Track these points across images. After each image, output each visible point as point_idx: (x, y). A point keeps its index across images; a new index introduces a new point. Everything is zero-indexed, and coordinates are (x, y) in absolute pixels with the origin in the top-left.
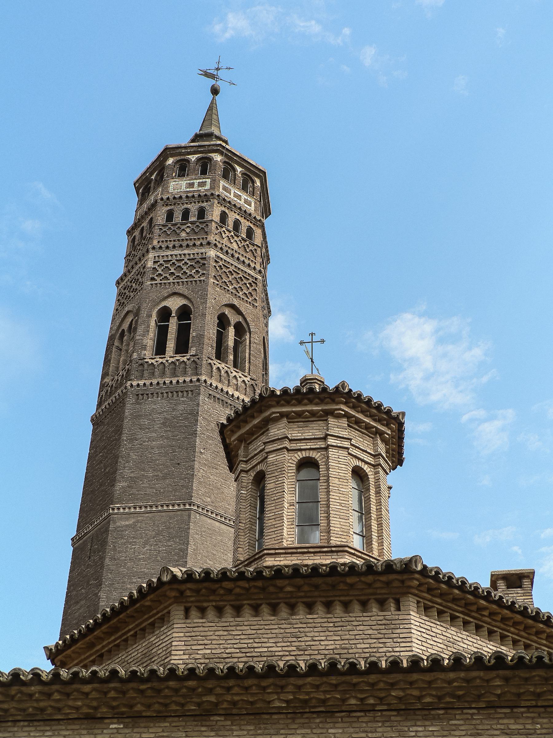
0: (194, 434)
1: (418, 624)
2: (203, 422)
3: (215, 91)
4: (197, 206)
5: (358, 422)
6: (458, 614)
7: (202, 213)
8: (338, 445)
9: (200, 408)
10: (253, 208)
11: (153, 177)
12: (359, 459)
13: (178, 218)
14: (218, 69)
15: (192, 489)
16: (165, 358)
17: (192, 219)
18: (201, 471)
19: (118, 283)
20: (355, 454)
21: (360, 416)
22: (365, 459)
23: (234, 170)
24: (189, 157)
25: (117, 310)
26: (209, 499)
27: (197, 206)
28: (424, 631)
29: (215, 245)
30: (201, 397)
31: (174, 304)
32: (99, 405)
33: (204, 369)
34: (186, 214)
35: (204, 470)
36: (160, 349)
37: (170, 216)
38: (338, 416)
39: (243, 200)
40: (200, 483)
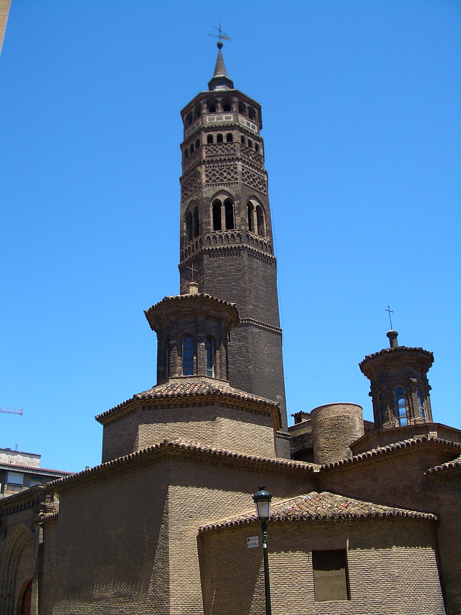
3: (220, 46)
4: (227, 132)
7: (230, 137)
10: (256, 131)
11: (193, 110)
13: (215, 141)
14: (220, 31)
16: (222, 232)
17: (225, 141)
19: (181, 179)
23: (245, 106)
24: (217, 99)
25: (183, 198)
27: (227, 132)
29: (241, 159)
31: (222, 198)
32: (182, 257)
33: (244, 239)
34: (220, 137)
36: (217, 226)
37: (210, 139)
39: (251, 126)
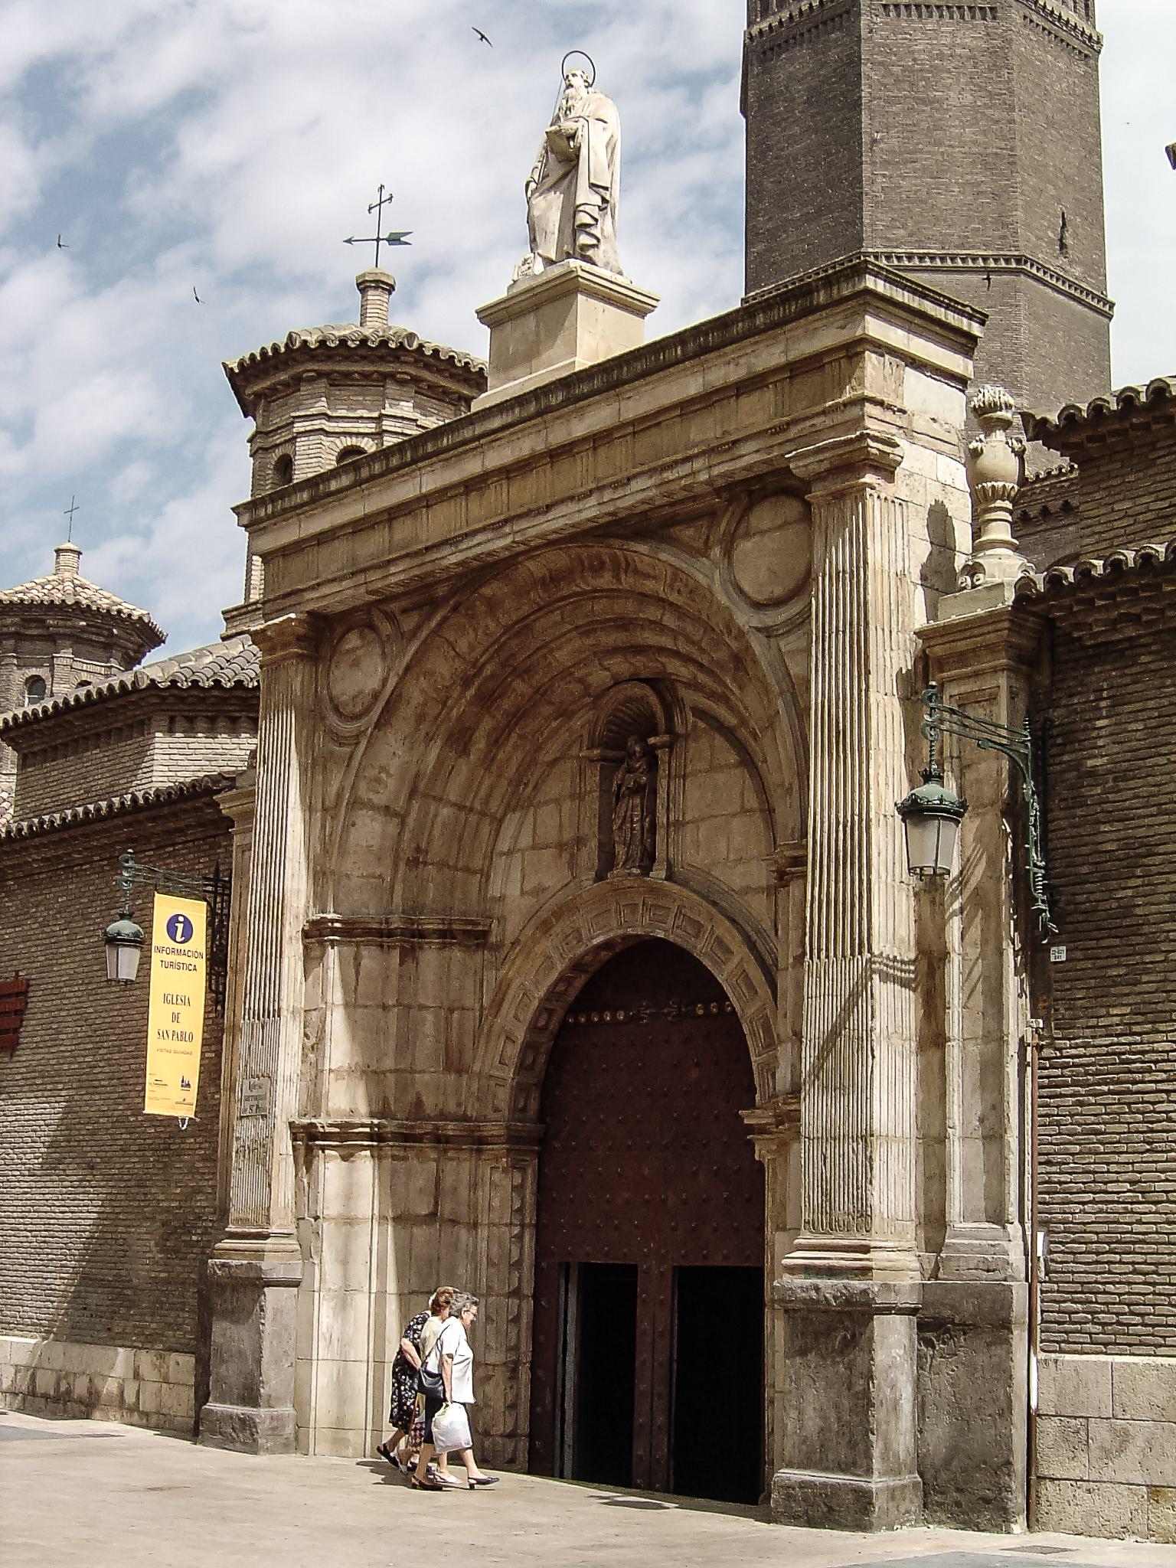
0: (857, 105)
1: (166, 746)
2: (872, 74)
5: (347, 375)
6: (237, 714)
8: (308, 428)
9: (864, 47)
12: (351, 434)
15: (862, 223)
18: (880, 179)
20: (342, 430)
21: (343, 367)
22: (361, 431)
26: (902, 232)
28: (175, 751)
30: (864, 21)
35: (884, 176)
38: (311, 380)
40: (877, 204)
